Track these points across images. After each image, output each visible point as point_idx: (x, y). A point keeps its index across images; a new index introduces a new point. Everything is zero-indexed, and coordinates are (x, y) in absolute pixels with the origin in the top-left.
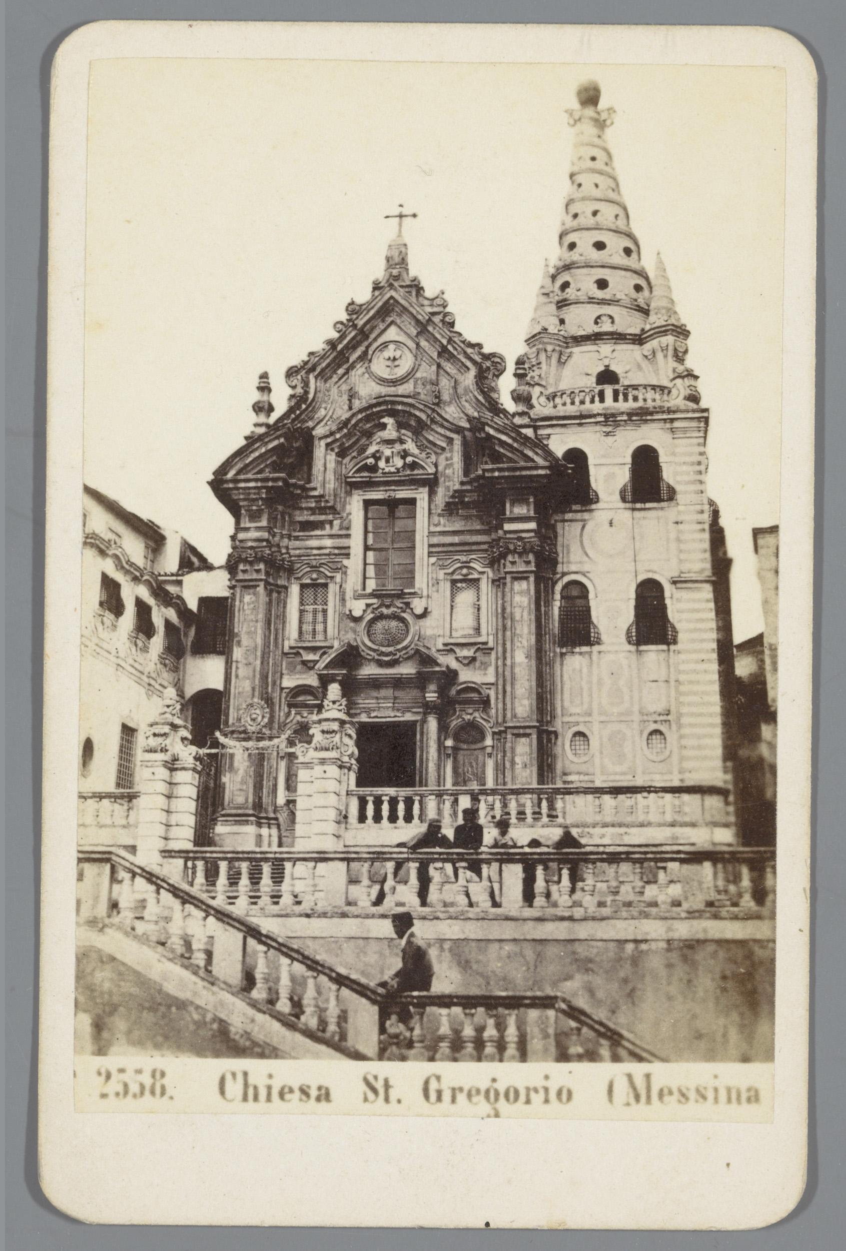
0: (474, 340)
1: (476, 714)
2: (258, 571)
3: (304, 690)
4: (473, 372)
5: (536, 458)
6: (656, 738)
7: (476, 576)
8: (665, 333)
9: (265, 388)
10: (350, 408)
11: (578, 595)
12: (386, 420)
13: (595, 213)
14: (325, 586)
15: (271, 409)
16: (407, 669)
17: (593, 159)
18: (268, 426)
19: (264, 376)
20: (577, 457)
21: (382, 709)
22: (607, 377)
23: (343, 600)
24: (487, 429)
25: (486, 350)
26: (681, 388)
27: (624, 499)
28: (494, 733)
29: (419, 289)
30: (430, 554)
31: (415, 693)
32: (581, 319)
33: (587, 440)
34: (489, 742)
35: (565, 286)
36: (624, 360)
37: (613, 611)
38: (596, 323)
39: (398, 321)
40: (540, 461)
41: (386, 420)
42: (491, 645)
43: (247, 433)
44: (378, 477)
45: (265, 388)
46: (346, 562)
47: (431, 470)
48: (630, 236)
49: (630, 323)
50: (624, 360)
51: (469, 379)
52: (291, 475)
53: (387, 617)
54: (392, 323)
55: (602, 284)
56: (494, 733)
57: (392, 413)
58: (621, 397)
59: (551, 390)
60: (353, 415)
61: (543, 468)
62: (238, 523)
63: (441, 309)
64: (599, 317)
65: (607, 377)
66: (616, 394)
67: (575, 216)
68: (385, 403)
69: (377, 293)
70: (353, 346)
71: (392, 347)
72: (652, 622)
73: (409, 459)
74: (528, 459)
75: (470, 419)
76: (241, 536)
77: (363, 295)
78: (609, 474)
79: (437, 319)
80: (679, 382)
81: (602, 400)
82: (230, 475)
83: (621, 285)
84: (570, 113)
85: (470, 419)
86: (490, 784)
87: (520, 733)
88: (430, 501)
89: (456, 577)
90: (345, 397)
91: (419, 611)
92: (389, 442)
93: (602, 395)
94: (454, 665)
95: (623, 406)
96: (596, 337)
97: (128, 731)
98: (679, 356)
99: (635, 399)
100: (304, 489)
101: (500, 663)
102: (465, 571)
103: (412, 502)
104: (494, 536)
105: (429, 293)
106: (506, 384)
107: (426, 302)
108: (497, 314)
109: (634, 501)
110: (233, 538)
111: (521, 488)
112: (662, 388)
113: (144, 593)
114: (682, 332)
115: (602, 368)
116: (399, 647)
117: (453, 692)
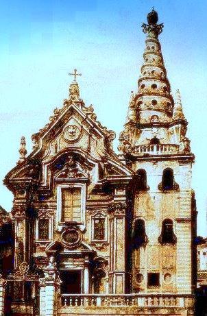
3: (41, 258)
10: (56, 152)
11: (140, 224)
15: (25, 152)
16: (78, 251)
19: (23, 138)
20: (142, 173)
21: (70, 265)
23: (54, 225)
30: (87, 209)
34: (107, 277)
37: (153, 231)
45: (23, 144)
49: (163, 118)
50: (161, 134)
65: (155, 141)
68: (70, 150)
72: (168, 237)
73: (79, 172)
75: (102, 158)
77: (60, 106)
78: (154, 178)
79: (89, 117)
81: (153, 150)
84: (144, 25)
85: (102, 158)
86: (107, 294)
88: (87, 187)
98: (183, 133)
103: (79, 189)
104: (110, 202)
105: (87, 105)
106: (116, 145)
108: (114, 118)
110: (14, 202)
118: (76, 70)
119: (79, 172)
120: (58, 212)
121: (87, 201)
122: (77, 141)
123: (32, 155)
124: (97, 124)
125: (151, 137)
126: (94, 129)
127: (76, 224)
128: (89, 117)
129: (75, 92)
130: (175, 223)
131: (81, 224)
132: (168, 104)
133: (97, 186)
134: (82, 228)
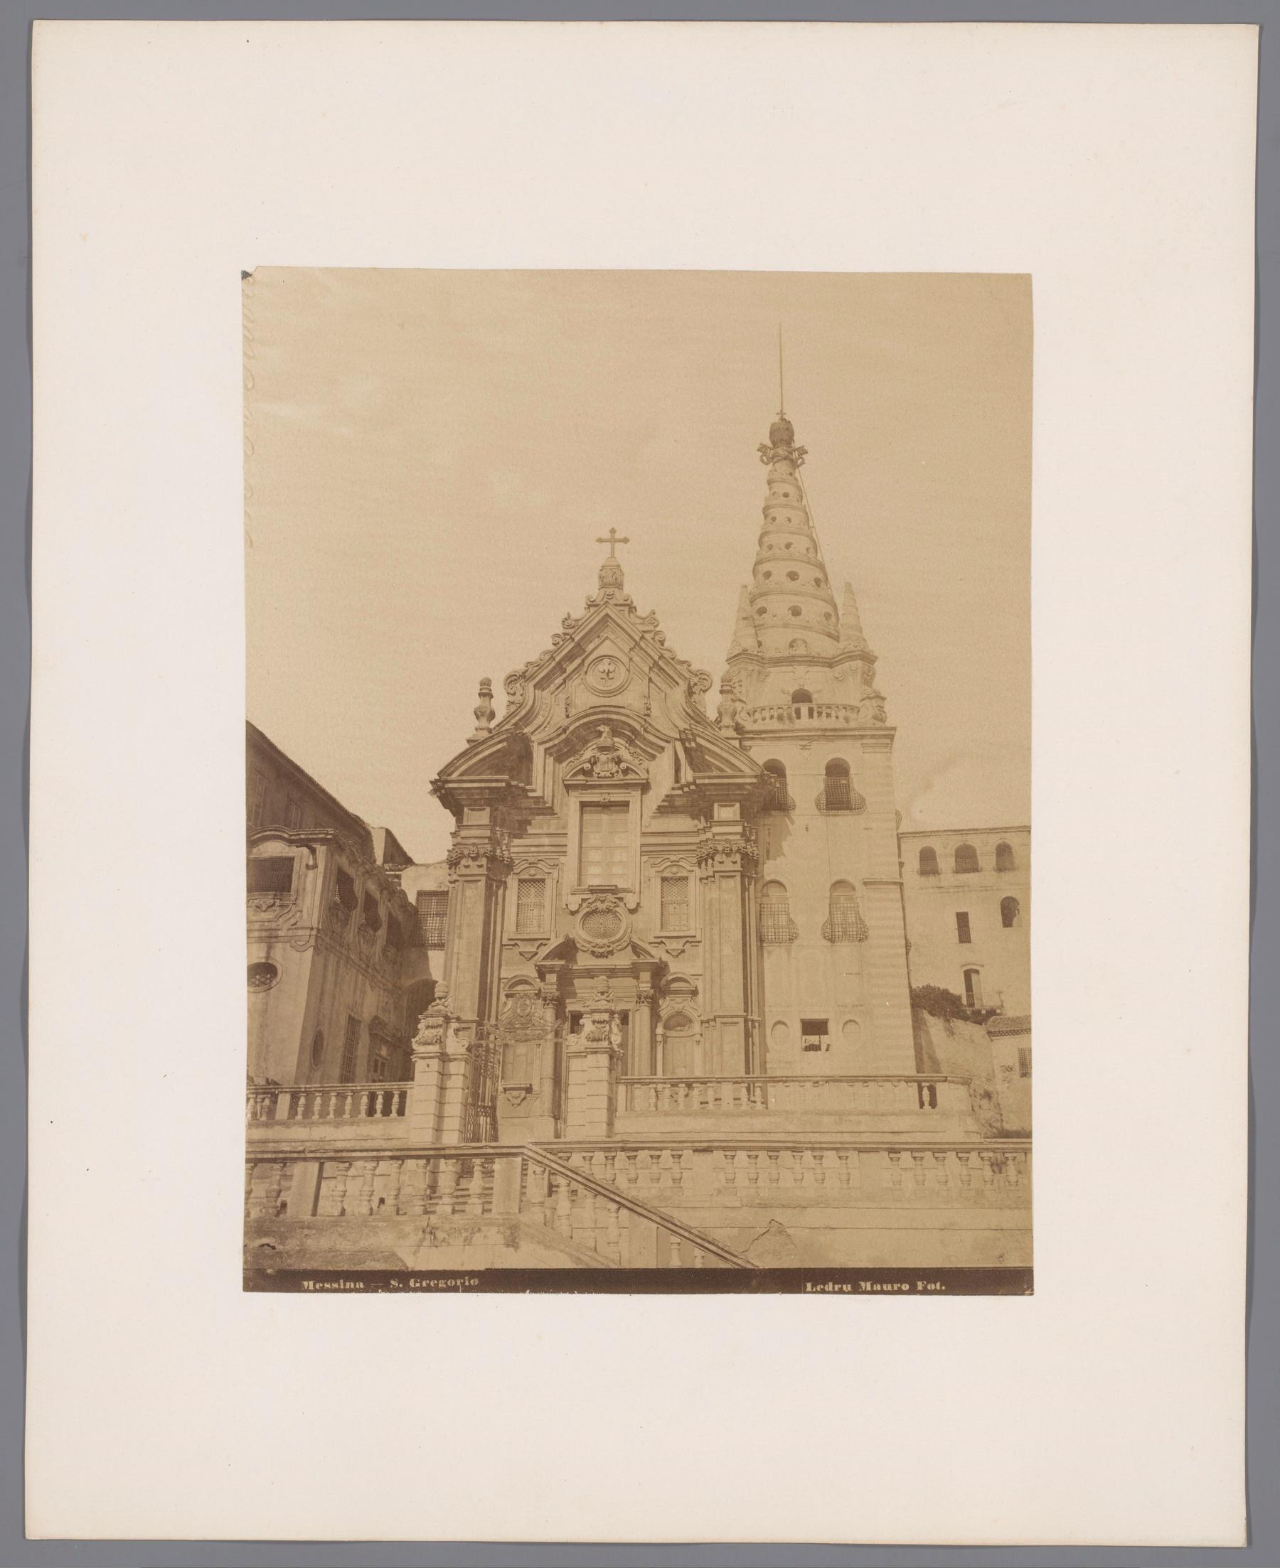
0: (681, 657)
1: (685, 1003)
2: (481, 866)
4: (683, 686)
5: (743, 767)
6: (851, 1027)
7: (684, 874)
8: (852, 658)
9: (486, 694)
12: (601, 728)
13: (788, 546)
14: (543, 881)
15: (492, 715)
17: (786, 495)
18: (490, 731)
19: (486, 683)
20: (776, 769)
22: (802, 696)
23: (559, 895)
24: (699, 740)
25: (694, 667)
26: (869, 709)
27: (818, 805)
28: (702, 1022)
29: (632, 609)
30: (642, 853)
31: (630, 981)
32: (776, 641)
33: (786, 753)
35: (762, 611)
36: (813, 679)
38: (791, 646)
39: (612, 637)
40: (748, 771)
41: (601, 728)
42: (698, 938)
43: (470, 735)
44: (593, 780)
45: (486, 694)
46: (562, 859)
47: (644, 775)
48: (821, 567)
50: (813, 679)
51: (678, 694)
52: (512, 778)
53: (602, 912)
54: (607, 638)
55: (796, 612)
56: (702, 1022)
57: (607, 722)
58: (815, 714)
59: (749, 707)
60: (571, 724)
61: (751, 777)
62: (459, 820)
63: (651, 628)
64: (794, 641)
66: (811, 711)
67: (770, 547)
69: (592, 610)
70: (570, 657)
71: (606, 661)
73: (623, 765)
74: (733, 766)
76: (463, 833)
77: (579, 612)
79: (648, 636)
80: (867, 702)
81: (799, 717)
82: (454, 776)
83: (813, 610)
87: (725, 1020)
89: (665, 875)
90: (563, 705)
91: (632, 906)
92: (603, 749)
93: (798, 712)
94: (665, 957)
95: (816, 723)
96: (791, 661)
97: (353, 1023)
99: (829, 715)
100: (525, 791)
101: (708, 956)
102: (674, 869)
104: (703, 837)
105: (642, 611)
107: (638, 621)
109: (828, 809)
111: (727, 794)
112: (852, 708)
113: (372, 886)
114: (868, 659)
115: (797, 688)
116: (613, 939)
117: (663, 982)
118: (613, 531)
119: (623, 765)
120: (570, 861)
121: (644, 834)
122: (619, 690)
123: (507, 719)
124: (667, 655)
125: (792, 688)
126: (663, 666)
127: (614, 890)
128: (648, 636)
129: (611, 579)
130: (858, 885)
131: (624, 890)
132: (828, 616)
133: (669, 798)
134: (631, 901)
